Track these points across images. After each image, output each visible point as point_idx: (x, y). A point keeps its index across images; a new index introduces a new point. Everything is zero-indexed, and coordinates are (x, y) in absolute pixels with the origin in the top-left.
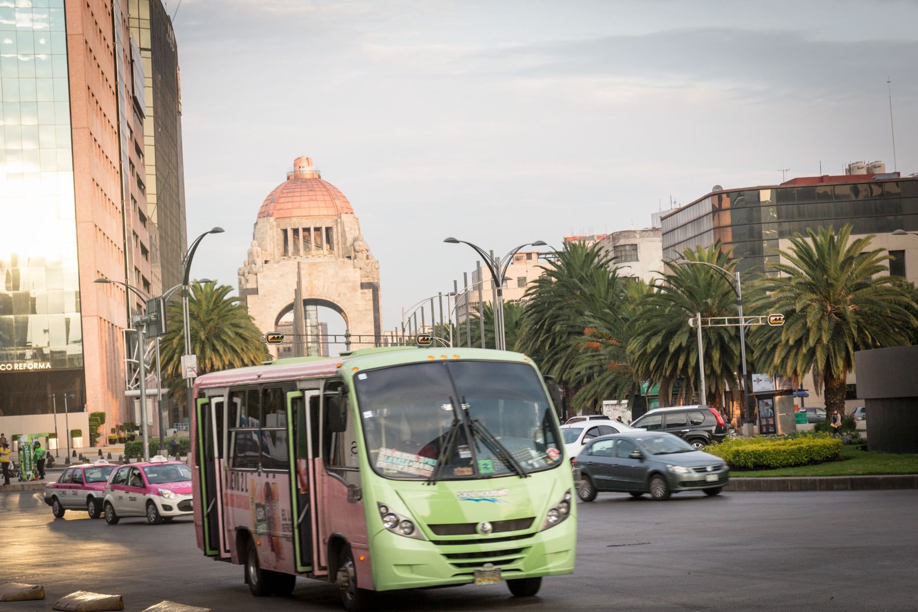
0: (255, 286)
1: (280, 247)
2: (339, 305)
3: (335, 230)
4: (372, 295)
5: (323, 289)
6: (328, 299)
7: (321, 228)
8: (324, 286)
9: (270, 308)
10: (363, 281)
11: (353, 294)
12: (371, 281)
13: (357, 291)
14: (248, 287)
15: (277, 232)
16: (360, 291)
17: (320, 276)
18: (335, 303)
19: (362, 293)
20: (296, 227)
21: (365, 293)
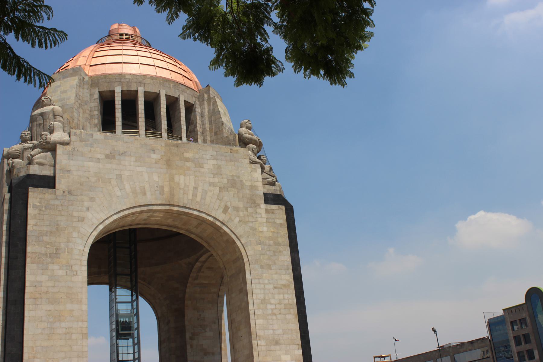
0: (47, 172)
1: (96, 121)
2: (224, 228)
3: (198, 110)
5: (195, 195)
8: (196, 188)
9: (82, 219)
12: (278, 193)
13: (259, 205)
14: (31, 172)
15: (91, 95)
16: (263, 206)
17: (189, 169)
18: (218, 223)
19: (267, 211)
20: (133, 88)
21: (273, 211)
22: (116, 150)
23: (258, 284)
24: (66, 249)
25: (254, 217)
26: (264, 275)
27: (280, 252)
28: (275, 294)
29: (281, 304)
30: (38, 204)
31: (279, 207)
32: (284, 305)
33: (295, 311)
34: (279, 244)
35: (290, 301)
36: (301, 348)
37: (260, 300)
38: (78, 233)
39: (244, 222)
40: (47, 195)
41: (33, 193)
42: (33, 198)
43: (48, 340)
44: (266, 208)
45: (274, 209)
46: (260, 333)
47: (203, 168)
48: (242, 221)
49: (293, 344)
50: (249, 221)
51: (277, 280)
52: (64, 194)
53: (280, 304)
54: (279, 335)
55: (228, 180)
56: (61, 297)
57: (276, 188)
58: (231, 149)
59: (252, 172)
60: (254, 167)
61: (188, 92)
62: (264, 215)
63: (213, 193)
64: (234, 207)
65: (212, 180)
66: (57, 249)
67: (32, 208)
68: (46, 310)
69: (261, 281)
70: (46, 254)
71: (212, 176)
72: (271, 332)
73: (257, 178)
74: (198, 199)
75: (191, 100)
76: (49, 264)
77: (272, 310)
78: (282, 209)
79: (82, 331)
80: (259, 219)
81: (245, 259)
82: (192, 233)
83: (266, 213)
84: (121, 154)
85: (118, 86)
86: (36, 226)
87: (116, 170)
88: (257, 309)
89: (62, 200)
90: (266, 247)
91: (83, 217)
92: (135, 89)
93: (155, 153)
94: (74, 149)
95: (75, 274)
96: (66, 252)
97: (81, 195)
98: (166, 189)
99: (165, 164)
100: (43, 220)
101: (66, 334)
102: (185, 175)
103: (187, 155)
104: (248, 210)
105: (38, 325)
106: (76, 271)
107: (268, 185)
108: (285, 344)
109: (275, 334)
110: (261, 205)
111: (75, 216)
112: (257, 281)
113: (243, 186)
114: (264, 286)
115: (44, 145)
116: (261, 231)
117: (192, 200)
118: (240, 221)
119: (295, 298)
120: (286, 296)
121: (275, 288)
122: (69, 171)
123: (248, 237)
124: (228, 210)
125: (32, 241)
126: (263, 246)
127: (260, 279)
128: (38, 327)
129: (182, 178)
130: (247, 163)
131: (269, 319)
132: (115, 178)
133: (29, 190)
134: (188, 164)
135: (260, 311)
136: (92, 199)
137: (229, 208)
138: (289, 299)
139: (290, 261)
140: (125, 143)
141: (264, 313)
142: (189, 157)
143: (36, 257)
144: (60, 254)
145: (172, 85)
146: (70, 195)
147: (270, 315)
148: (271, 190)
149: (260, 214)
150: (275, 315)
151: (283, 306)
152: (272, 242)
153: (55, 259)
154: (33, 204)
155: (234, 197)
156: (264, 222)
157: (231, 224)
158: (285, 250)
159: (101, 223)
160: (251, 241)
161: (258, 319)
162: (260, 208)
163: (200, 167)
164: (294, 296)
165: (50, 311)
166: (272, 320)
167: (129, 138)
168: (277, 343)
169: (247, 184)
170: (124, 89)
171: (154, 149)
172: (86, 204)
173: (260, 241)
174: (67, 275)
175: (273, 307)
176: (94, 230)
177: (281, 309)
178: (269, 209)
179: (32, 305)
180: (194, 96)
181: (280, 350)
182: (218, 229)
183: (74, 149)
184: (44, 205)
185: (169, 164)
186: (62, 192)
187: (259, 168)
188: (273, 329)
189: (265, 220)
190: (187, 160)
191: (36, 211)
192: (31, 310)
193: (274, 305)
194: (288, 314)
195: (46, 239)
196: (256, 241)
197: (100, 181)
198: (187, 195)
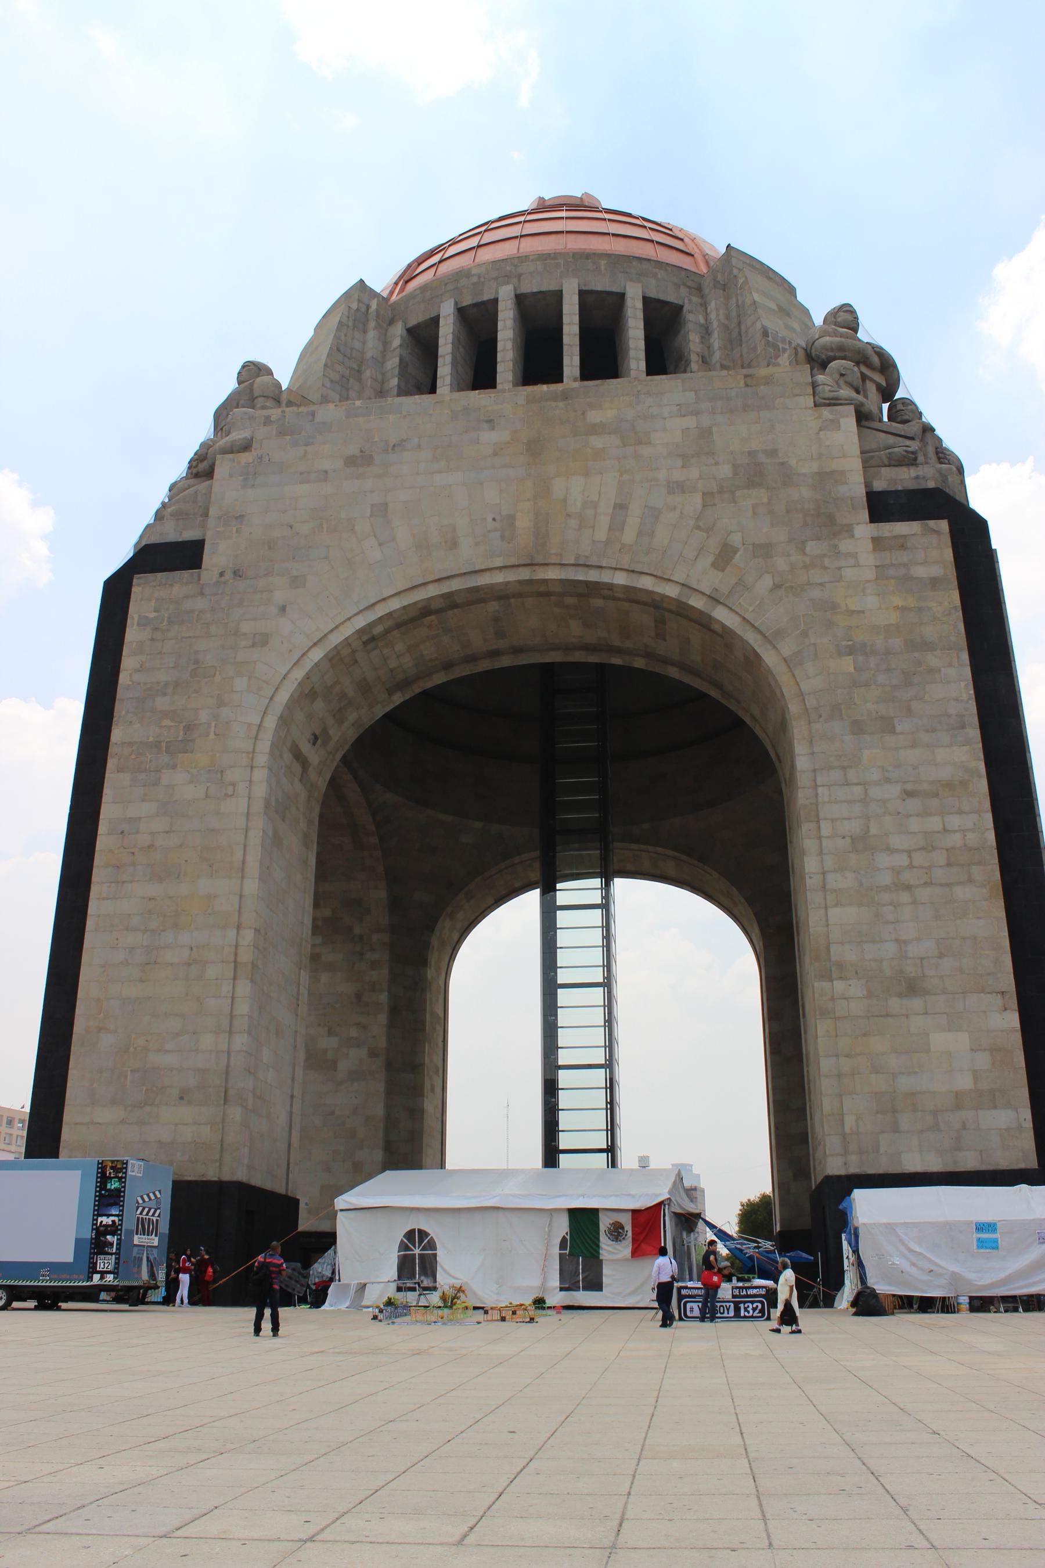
0: (190, 535)
2: (721, 614)
4: (949, 554)
5: (616, 526)
6: (646, 583)
7: (621, 297)
8: (621, 507)
10: (879, 486)
11: (814, 548)
12: (931, 485)
13: (848, 530)
15: (386, 344)
16: (865, 530)
18: (697, 602)
19: (877, 543)
21: (901, 543)
22: (376, 439)
23: (843, 785)
24: (213, 724)
25: (827, 568)
26: (866, 753)
27: (931, 671)
28: (908, 816)
29: (934, 848)
30: (153, 615)
31: (927, 524)
32: (945, 852)
33: (991, 870)
34: (927, 646)
35: (970, 836)
36: (1016, 1006)
37: (848, 840)
38: (250, 678)
39: (792, 587)
40: (176, 589)
41: (143, 588)
42: (142, 599)
43: (142, 981)
44: (876, 534)
45: (905, 536)
46: (843, 953)
47: (649, 443)
48: (783, 587)
49: (983, 992)
50: (808, 584)
51: (915, 768)
52: (223, 579)
53: (929, 847)
54: (922, 959)
55: (735, 467)
56: (186, 861)
57: (920, 473)
58: (746, 376)
59: (821, 433)
60: (831, 417)
61: (659, 276)
62: (867, 557)
63: (681, 513)
64: (753, 544)
65: (678, 475)
66: (188, 728)
67: (135, 627)
68: (144, 898)
69: (852, 775)
70: (157, 745)
71: (679, 462)
72: (890, 949)
73: (842, 446)
74: (629, 536)
75: (671, 297)
76: (163, 771)
77: (897, 871)
78: (938, 532)
79: (236, 954)
80: (848, 573)
81: (793, 708)
82: (665, 661)
83: (875, 550)
84: (390, 449)
85: (451, 298)
86: (139, 671)
87: (372, 492)
88: (835, 871)
89: (216, 594)
90: (873, 662)
91: (267, 634)
92: (492, 297)
93: (493, 429)
94: (261, 458)
95: (230, 794)
96: (212, 736)
97: (266, 575)
98: (524, 523)
99: (522, 454)
100: (160, 653)
101: (189, 965)
102: (587, 474)
103: (594, 416)
104: (808, 549)
105: (117, 939)
106: (234, 785)
107: (889, 466)
108: (944, 993)
109: (907, 958)
110: (855, 526)
111: (245, 634)
112: (836, 775)
113: (788, 478)
114: (866, 790)
115: (196, 466)
116: (858, 612)
117: (607, 543)
118: (777, 587)
119: (992, 825)
120: (955, 821)
121: (909, 794)
122: (242, 516)
123: (805, 634)
124: (732, 558)
125: (128, 712)
126: (861, 659)
127: (851, 767)
128: (117, 944)
129: (577, 483)
130: (806, 408)
131: (884, 905)
132: (368, 514)
133: (135, 581)
134: (597, 442)
135: (846, 878)
136: (297, 582)
137: (735, 551)
138: (968, 830)
139: (969, 699)
140: (405, 416)
141: (861, 885)
142: (601, 422)
143: (132, 754)
144: (193, 741)
145: (603, 262)
146: (239, 578)
147: (886, 888)
148: (901, 480)
149: (854, 555)
150: (908, 888)
151: (940, 858)
152: (897, 643)
153: (180, 755)
154: (139, 616)
155: (755, 513)
156: (868, 581)
157: (742, 598)
158: (950, 665)
159: (315, 644)
160: (815, 644)
161: (836, 905)
162: (853, 536)
163: (640, 443)
164: (988, 819)
165: (153, 899)
166: (895, 905)
167: (419, 401)
168: (912, 988)
169: (803, 471)
170: (464, 304)
171: (492, 418)
172: (280, 596)
173: (850, 643)
174: (206, 796)
175: (902, 860)
176: (295, 664)
177: (930, 867)
178: (888, 535)
179: (109, 884)
180: (685, 285)
181: (926, 1013)
182: (703, 622)
183: (261, 458)
184: (166, 615)
185: (535, 449)
186: (216, 573)
187: (847, 416)
188: (897, 940)
189: (870, 574)
190: (597, 429)
191: (145, 634)
192: (104, 899)
193: (905, 856)
194: (962, 883)
195: (162, 703)
196: (837, 645)
197: (325, 530)
198: (591, 530)
